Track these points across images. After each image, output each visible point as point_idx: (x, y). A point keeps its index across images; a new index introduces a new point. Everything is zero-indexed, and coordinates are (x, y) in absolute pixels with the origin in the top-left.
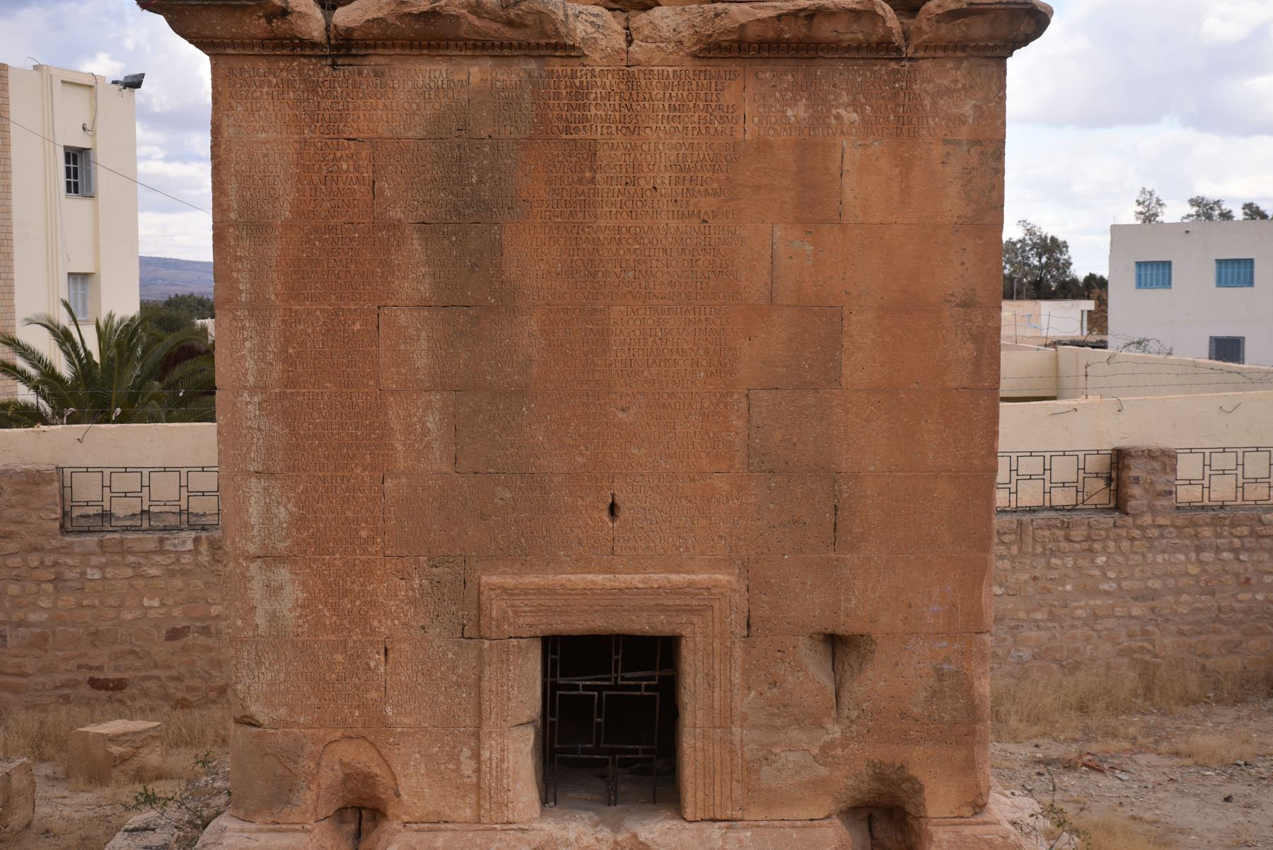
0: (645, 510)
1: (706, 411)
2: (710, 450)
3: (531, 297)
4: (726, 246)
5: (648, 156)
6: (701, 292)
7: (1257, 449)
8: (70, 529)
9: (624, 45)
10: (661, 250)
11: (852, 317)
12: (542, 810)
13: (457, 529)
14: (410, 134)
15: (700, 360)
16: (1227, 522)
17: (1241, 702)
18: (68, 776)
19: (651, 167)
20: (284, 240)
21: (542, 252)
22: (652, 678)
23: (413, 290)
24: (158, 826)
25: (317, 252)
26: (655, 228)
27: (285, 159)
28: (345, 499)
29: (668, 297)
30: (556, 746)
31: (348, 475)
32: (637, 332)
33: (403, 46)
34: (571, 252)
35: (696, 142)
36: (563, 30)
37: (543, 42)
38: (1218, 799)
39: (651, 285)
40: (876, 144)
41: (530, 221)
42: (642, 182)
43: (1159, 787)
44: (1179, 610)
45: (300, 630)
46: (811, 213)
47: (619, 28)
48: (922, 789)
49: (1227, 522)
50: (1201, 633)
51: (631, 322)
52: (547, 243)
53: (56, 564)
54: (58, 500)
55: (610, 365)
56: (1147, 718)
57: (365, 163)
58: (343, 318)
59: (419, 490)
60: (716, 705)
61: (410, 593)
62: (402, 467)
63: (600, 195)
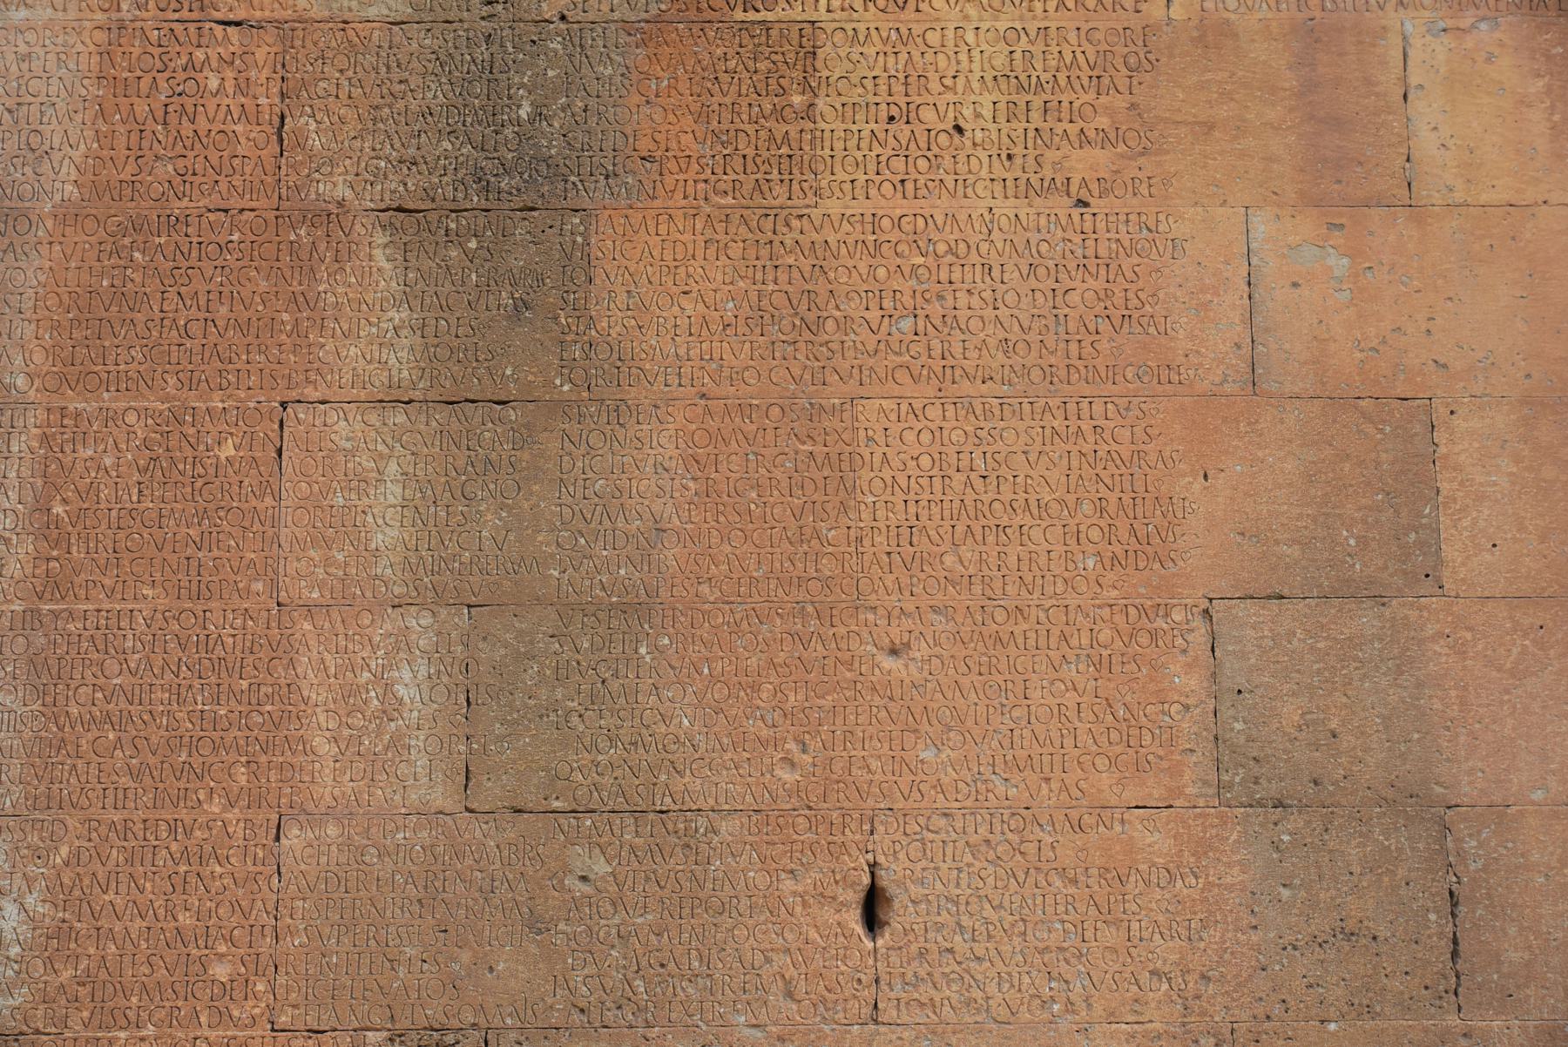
0: (957, 904)
1: (1105, 653)
2: (1118, 749)
3: (661, 378)
4: (1135, 260)
5: (940, 56)
6: (1079, 363)
10: (978, 268)
11: (1456, 421)
13: (466, 956)
14: (372, 12)
15: (1083, 528)
19: (948, 82)
20: (57, 248)
21: (689, 276)
23: (369, 363)
25: (138, 277)
26: (962, 217)
27: (72, 66)
28: (177, 880)
29: (998, 378)
31: (188, 821)
32: (925, 461)
34: (759, 276)
35: (1053, 25)
39: (957, 349)
40: (1483, 26)
41: (657, 203)
42: (928, 114)
46: (1339, 182)
51: (910, 436)
52: (700, 253)
55: (860, 540)
57: (265, 73)
58: (192, 431)
59: (371, 856)
62: (328, 798)
63: (827, 144)
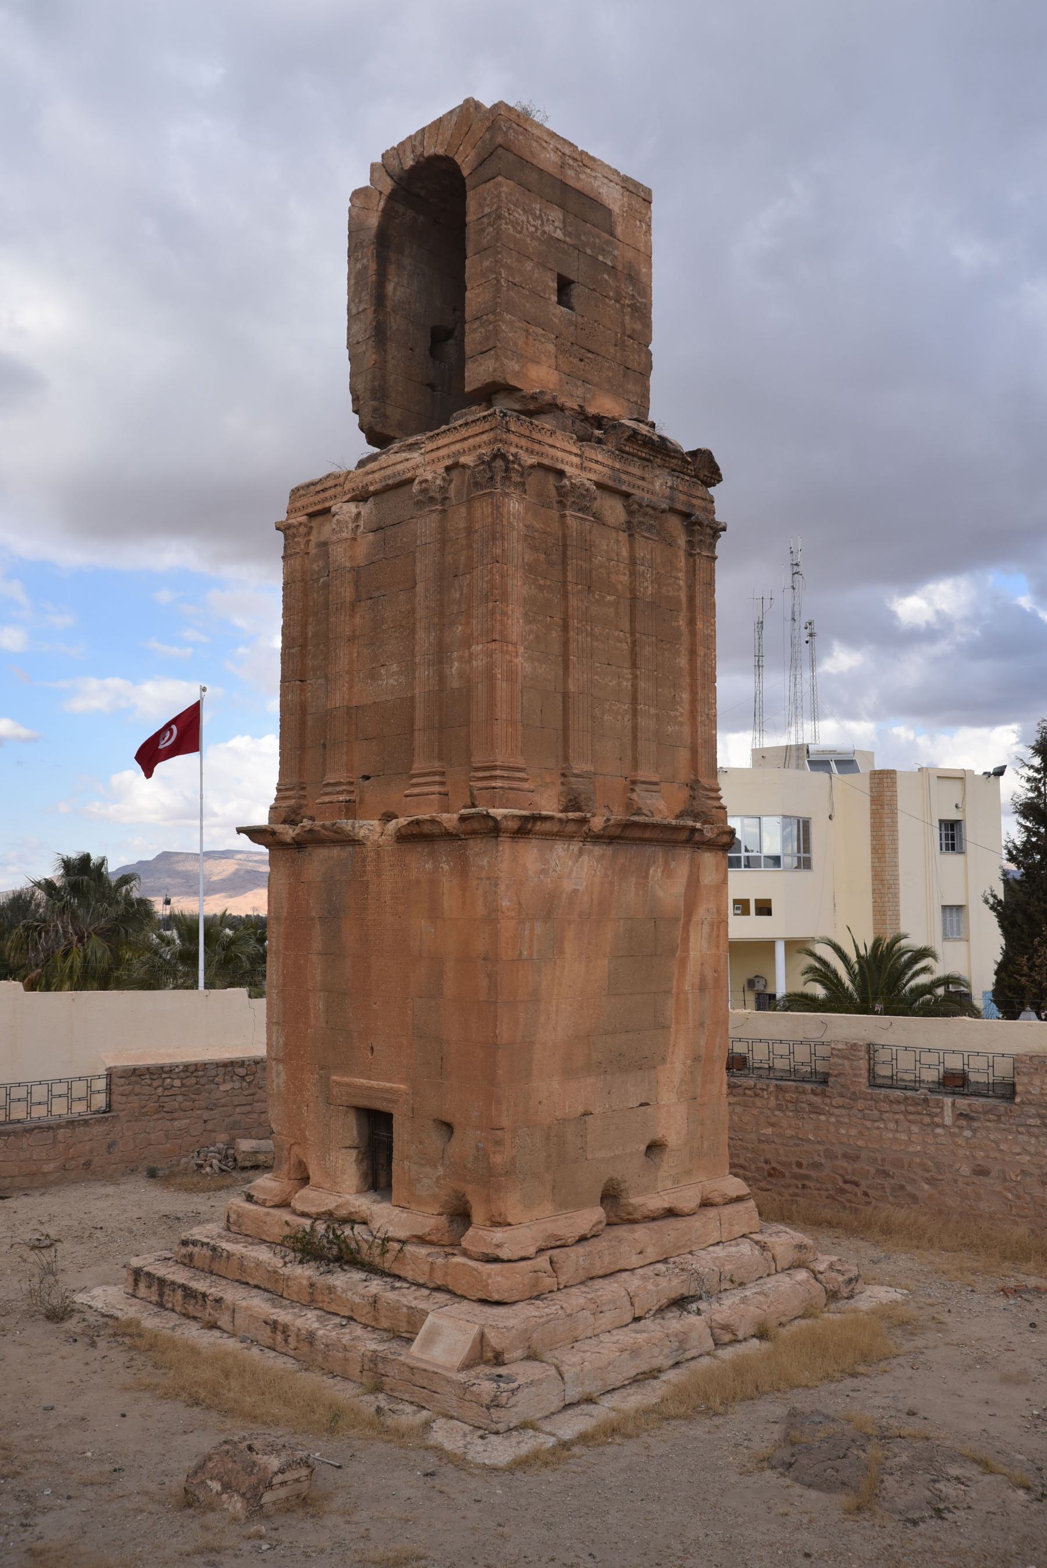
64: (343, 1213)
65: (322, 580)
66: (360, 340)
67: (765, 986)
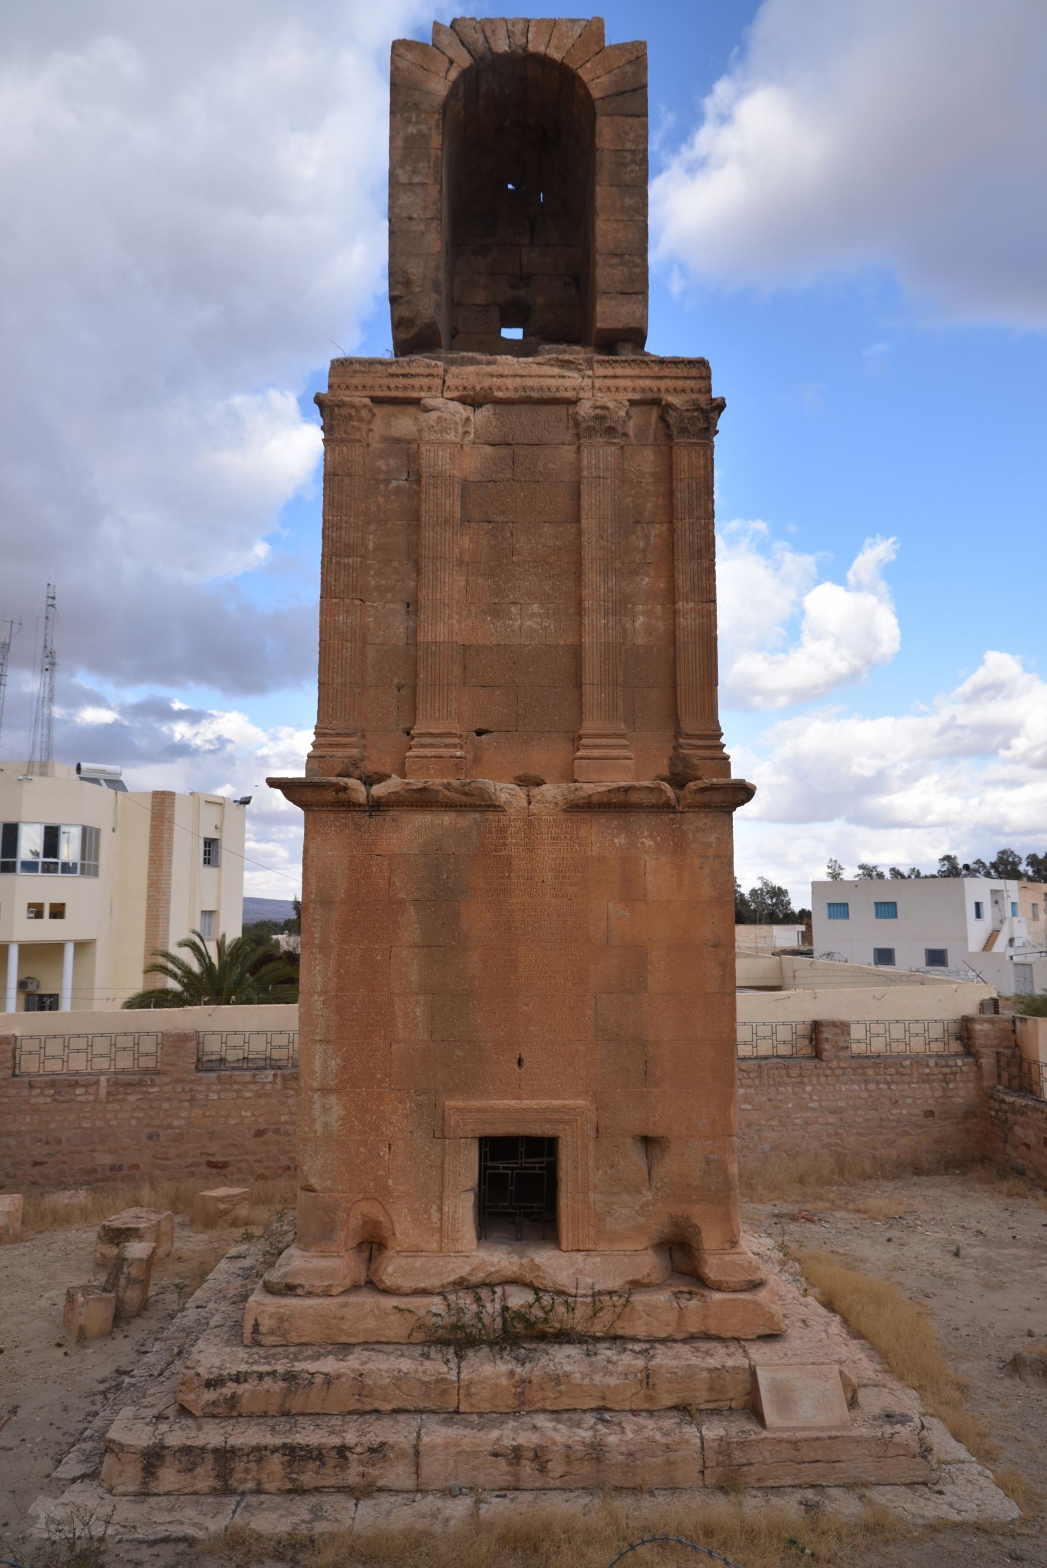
7: (897, 1022)
8: (201, 1068)
9: (526, 805)
12: (478, 1244)
14: (410, 852)
16: (882, 1066)
17: (897, 1178)
18: (192, 1222)
22: (542, 1163)
24: (249, 1254)
30: (487, 1204)
33: (408, 806)
36: (494, 797)
37: (483, 803)
38: (883, 1240)
42: (536, 878)
43: (848, 1233)
44: (857, 1120)
45: (341, 1133)
47: (524, 796)
48: (700, 1232)
49: (882, 1066)
50: (871, 1134)
53: (192, 1090)
54: (195, 1051)
56: (841, 1188)
60: (579, 1179)
61: (404, 1111)
64: (480, 1276)
65: (394, 483)
66: (415, 216)
67: (38, 987)
